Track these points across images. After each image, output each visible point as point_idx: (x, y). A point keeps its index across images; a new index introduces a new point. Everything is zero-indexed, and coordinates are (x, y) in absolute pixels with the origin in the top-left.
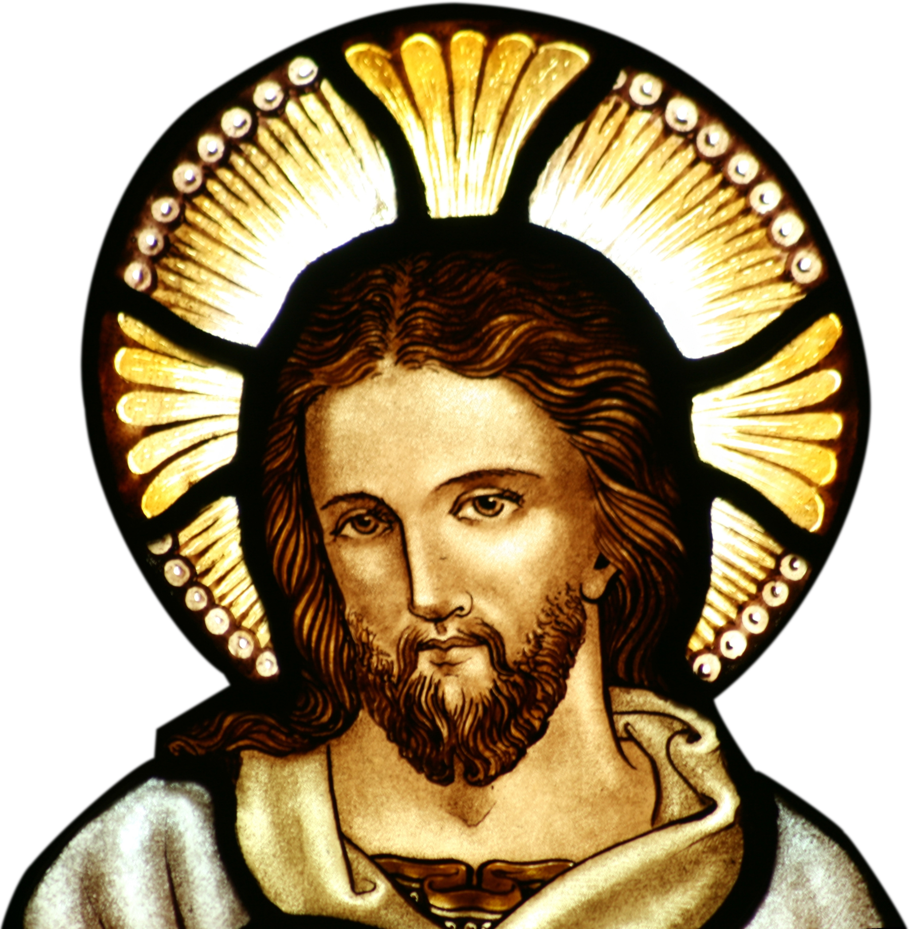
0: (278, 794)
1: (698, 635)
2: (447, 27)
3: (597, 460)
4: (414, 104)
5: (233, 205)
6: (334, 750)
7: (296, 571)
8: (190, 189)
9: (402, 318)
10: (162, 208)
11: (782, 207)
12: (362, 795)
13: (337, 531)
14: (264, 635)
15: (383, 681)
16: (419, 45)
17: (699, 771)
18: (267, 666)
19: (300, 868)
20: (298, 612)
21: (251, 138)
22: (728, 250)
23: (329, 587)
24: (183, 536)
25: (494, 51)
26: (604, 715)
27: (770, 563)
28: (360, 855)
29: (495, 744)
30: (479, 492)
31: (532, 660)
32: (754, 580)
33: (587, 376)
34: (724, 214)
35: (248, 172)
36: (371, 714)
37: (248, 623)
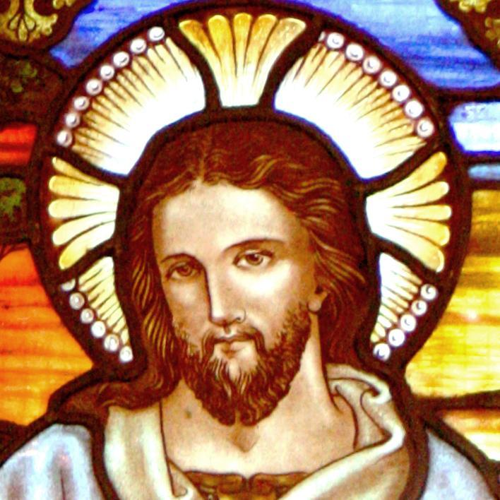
0: (130, 433)
1: (376, 333)
2: (232, 11)
3: (314, 231)
4: (214, 49)
5: (118, 101)
6: (164, 406)
7: (145, 297)
8: (95, 93)
9: (207, 158)
10: (80, 102)
11: (411, 98)
12: (179, 432)
13: (169, 275)
14: (125, 336)
15: (193, 363)
16: (218, 21)
17: (380, 414)
18: (126, 356)
19: (142, 481)
20: (146, 322)
21: (129, 67)
22: (383, 120)
23: (162, 306)
24: (82, 279)
25: (256, 23)
26: (323, 381)
27: (415, 290)
28: (178, 472)
29: (259, 399)
30: (249, 252)
31: (280, 349)
32: (406, 300)
33: (306, 186)
34: (380, 102)
35: (126, 84)
36: (187, 383)
37: (116, 330)
